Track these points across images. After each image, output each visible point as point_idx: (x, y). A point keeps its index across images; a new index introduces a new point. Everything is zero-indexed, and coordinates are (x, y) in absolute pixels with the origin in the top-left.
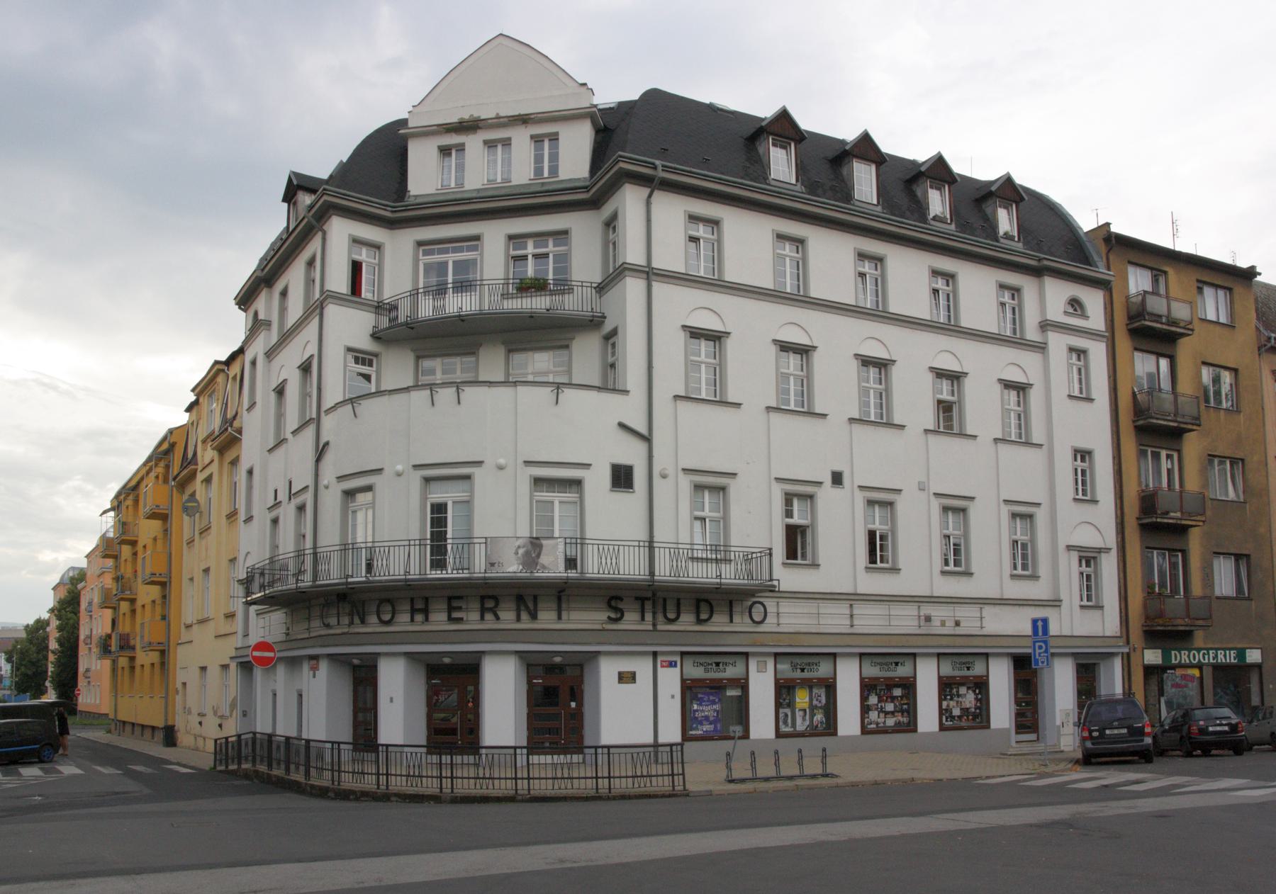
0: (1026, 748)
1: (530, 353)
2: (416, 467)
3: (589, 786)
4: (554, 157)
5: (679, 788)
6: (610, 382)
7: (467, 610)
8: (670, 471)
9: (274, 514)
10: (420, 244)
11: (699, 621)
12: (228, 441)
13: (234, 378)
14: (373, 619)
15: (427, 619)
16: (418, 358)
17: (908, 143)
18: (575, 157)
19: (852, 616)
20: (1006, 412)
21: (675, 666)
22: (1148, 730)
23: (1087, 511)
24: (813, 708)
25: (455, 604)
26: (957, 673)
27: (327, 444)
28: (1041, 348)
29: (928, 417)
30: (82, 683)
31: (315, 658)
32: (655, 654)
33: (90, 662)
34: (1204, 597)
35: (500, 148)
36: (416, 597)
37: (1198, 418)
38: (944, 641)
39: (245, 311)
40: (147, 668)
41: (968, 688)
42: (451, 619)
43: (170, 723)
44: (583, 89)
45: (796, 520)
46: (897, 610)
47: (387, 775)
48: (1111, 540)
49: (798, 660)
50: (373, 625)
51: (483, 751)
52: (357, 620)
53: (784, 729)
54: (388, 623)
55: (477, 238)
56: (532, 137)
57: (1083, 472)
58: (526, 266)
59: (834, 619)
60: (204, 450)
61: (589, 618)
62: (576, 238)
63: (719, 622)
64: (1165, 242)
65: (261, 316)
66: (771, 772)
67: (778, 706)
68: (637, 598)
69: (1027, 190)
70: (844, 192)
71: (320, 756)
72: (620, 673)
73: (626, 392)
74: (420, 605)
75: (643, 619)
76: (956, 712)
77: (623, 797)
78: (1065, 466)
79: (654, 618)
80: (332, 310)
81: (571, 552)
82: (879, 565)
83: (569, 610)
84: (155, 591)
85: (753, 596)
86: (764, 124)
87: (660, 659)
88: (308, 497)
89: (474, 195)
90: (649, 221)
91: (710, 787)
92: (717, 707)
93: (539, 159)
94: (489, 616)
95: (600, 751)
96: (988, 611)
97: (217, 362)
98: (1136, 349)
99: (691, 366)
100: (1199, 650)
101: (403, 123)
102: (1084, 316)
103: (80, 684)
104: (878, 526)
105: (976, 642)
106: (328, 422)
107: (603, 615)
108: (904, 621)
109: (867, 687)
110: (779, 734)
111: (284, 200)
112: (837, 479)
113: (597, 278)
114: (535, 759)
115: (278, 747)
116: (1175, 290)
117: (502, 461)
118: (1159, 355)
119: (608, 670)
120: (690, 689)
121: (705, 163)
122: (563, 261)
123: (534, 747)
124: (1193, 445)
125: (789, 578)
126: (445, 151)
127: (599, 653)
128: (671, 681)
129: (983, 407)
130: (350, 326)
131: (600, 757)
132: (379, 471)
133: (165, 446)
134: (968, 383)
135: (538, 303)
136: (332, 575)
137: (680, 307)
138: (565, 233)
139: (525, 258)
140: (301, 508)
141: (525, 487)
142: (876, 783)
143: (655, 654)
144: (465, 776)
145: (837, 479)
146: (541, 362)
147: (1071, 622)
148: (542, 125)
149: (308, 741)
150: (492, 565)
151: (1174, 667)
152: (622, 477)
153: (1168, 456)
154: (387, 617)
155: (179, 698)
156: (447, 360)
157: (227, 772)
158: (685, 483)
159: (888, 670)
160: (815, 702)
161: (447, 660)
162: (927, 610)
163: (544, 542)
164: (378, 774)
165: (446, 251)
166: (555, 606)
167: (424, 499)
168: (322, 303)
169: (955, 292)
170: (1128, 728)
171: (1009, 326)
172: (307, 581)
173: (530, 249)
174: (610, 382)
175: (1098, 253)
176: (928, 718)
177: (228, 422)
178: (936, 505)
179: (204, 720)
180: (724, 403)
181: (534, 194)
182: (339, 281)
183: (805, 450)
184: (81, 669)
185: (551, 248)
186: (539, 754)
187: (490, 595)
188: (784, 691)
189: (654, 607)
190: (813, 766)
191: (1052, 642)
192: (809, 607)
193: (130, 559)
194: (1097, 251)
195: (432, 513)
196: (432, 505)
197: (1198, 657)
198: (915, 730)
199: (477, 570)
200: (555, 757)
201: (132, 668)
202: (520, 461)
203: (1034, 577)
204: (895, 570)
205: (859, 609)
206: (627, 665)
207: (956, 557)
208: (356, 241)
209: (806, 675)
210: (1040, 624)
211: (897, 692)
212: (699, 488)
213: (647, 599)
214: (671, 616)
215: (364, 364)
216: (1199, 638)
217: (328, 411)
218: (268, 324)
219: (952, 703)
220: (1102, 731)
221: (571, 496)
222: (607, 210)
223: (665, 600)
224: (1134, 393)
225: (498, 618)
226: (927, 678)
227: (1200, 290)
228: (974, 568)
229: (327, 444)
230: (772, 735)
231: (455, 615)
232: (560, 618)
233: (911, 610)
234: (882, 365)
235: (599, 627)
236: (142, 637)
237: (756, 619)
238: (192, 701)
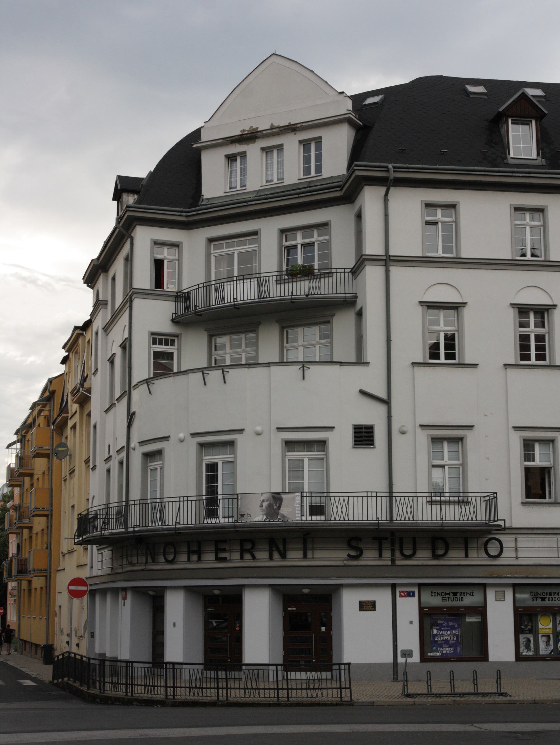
2: (194, 435)
7: (230, 551)
11: (435, 557)
15: (199, 559)
16: (210, 337)
21: (413, 596)
25: (221, 546)
31: (124, 589)
39: (92, 288)
42: (218, 559)
43: (50, 643)
49: (540, 590)
51: (244, 667)
53: (524, 652)
55: (255, 233)
61: (335, 556)
62: (335, 228)
63: (455, 557)
66: (470, 689)
67: (518, 631)
68: (374, 538)
72: (361, 602)
75: (380, 555)
79: (393, 554)
80: (137, 303)
81: (317, 501)
83: (313, 549)
90: (386, 215)
91: (375, 699)
94: (247, 556)
106: (135, 394)
107: (343, 554)
110: (519, 657)
114: (292, 675)
117: (259, 429)
119: (349, 600)
120: (427, 616)
123: (290, 664)
127: (341, 586)
128: (409, 609)
131: (343, 671)
132: (166, 438)
135: (300, 289)
138: (326, 225)
140: (121, 463)
141: (277, 448)
142: (535, 702)
143: (394, 587)
146: (306, 339)
150: (242, 516)
152: (363, 436)
154: (171, 557)
155: (57, 619)
157: (57, 685)
158: (423, 437)
163: (283, 496)
164: (126, 684)
166: (301, 546)
173: (299, 239)
185: (316, 237)
186: (295, 671)
187: (246, 539)
188: (525, 618)
201: (30, 590)
206: (367, 595)
212: (436, 440)
213: (386, 539)
214: (408, 552)
217: (137, 385)
221: (315, 454)
223: (401, 539)
225: (254, 557)
230: (511, 657)
232: (305, 556)
237: (493, 552)
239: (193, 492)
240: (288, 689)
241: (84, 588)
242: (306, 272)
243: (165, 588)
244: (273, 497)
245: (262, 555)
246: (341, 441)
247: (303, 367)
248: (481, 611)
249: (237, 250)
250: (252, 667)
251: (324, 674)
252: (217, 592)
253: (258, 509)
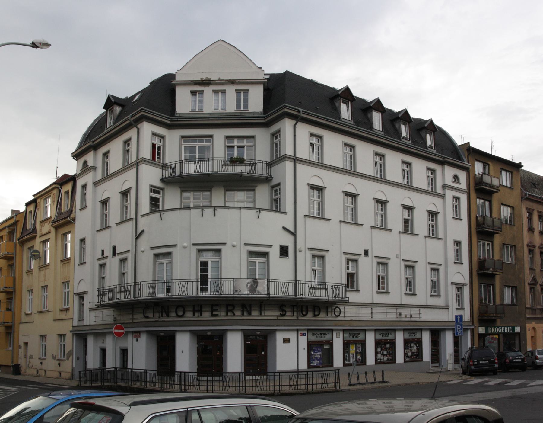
0: (436, 370)
1: (236, 192)
2: (194, 245)
3: (271, 389)
4: (246, 101)
6: (276, 206)
7: (220, 311)
8: (303, 249)
9: (102, 262)
10: (183, 137)
11: (315, 316)
12: (64, 222)
14: (173, 314)
15: (201, 315)
16: (182, 191)
18: (256, 102)
19: (372, 313)
20: (376, 214)
22: (496, 361)
23: (458, 267)
24: (356, 353)
25: (214, 308)
26: (411, 337)
28: (443, 196)
29: (400, 227)
32: (297, 330)
34: (500, 305)
35: (220, 94)
36: (196, 305)
37: (501, 228)
38: (406, 324)
41: (414, 344)
42: (213, 315)
44: (260, 70)
45: (351, 271)
47: (185, 385)
48: (467, 281)
50: (173, 317)
52: (164, 315)
54: (182, 316)
55: (211, 136)
56: (236, 90)
58: (234, 151)
59: (365, 314)
61: (271, 314)
63: (322, 316)
64: (489, 151)
65: (90, 164)
68: (291, 306)
69: (439, 128)
70: (369, 124)
72: (284, 339)
73: (286, 213)
76: (410, 354)
77: (318, 393)
78: (451, 247)
79: (297, 314)
83: (264, 310)
85: (335, 304)
86: (339, 93)
87: (299, 332)
88: (130, 257)
89: (208, 116)
90: (295, 135)
92: (320, 353)
93: (238, 101)
95: (276, 374)
96: (423, 311)
98: (478, 198)
99: (311, 202)
100: (498, 327)
102: (459, 183)
104: (381, 274)
105: (418, 324)
107: (278, 313)
108: (391, 315)
109: (378, 343)
112: (366, 253)
113: (268, 160)
114: (248, 378)
116: (492, 173)
117: (235, 243)
118: (486, 200)
119: (280, 337)
120: (311, 346)
121: (316, 110)
124: (497, 239)
125: (353, 297)
126: (193, 93)
127: (276, 330)
128: (303, 341)
129: (421, 222)
130: (151, 175)
131: (276, 377)
134: (415, 211)
136: (144, 294)
137: (308, 175)
138: (253, 137)
139: (233, 147)
141: (244, 255)
143: (297, 330)
145: (366, 253)
148: (241, 85)
150: (236, 291)
151: (489, 334)
153: (488, 244)
154: (181, 314)
156: (195, 193)
158: (309, 254)
159: (385, 336)
160: (357, 351)
161: (209, 333)
162: (400, 310)
163: (259, 281)
165: (195, 141)
167: (197, 259)
168: (138, 163)
169: (411, 171)
170: (489, 360)
171: (379, 173)
174: (276, 206)
175: (464, 155)
176: (400, 357)
178: (403, 264)
180: (323, 219)
182: (146, 153)
183: (355, 240)
185: (245, 143)
189: (297, 309)
191: (463, 324)
194: (464, 154)
195: (201, 266)
196: (201, 262)
197: (498, 330)
198: (395, 362)
199: (224, 293)
200: (257, 377)
202: (243, 243)
203: (439, 296)
204: (387, 293)
205: (375, 310)
206: (287, 335)
207: (410, 287)
208: (154, 134)
209: (355, 339)
210: (459, 317)
211: (388, 346)
214: (304, 313)
215: (157, 193)
216: (498, 322)
217: (143, 216)
219: (408, 351)
220: (478, 362)
222: (274, 128)
224: (477, 217)
225: (234, 314)
226: (400, 339)
227: (501, 172)
228: (417, 292)
231: (215, 313)
232: (261, 314)
233: (393, 311)
234: (354, 196)
235: (276, 318)
239: (193, 276)
240: (279, 386)
241: (122, 331)
242: (240, 161)
243: (176, 331)
244: (254, 281)
246: (274, 253)
247: (259, 211)
248: (331, 343)
250: (233, 374)
253: (245, 288)
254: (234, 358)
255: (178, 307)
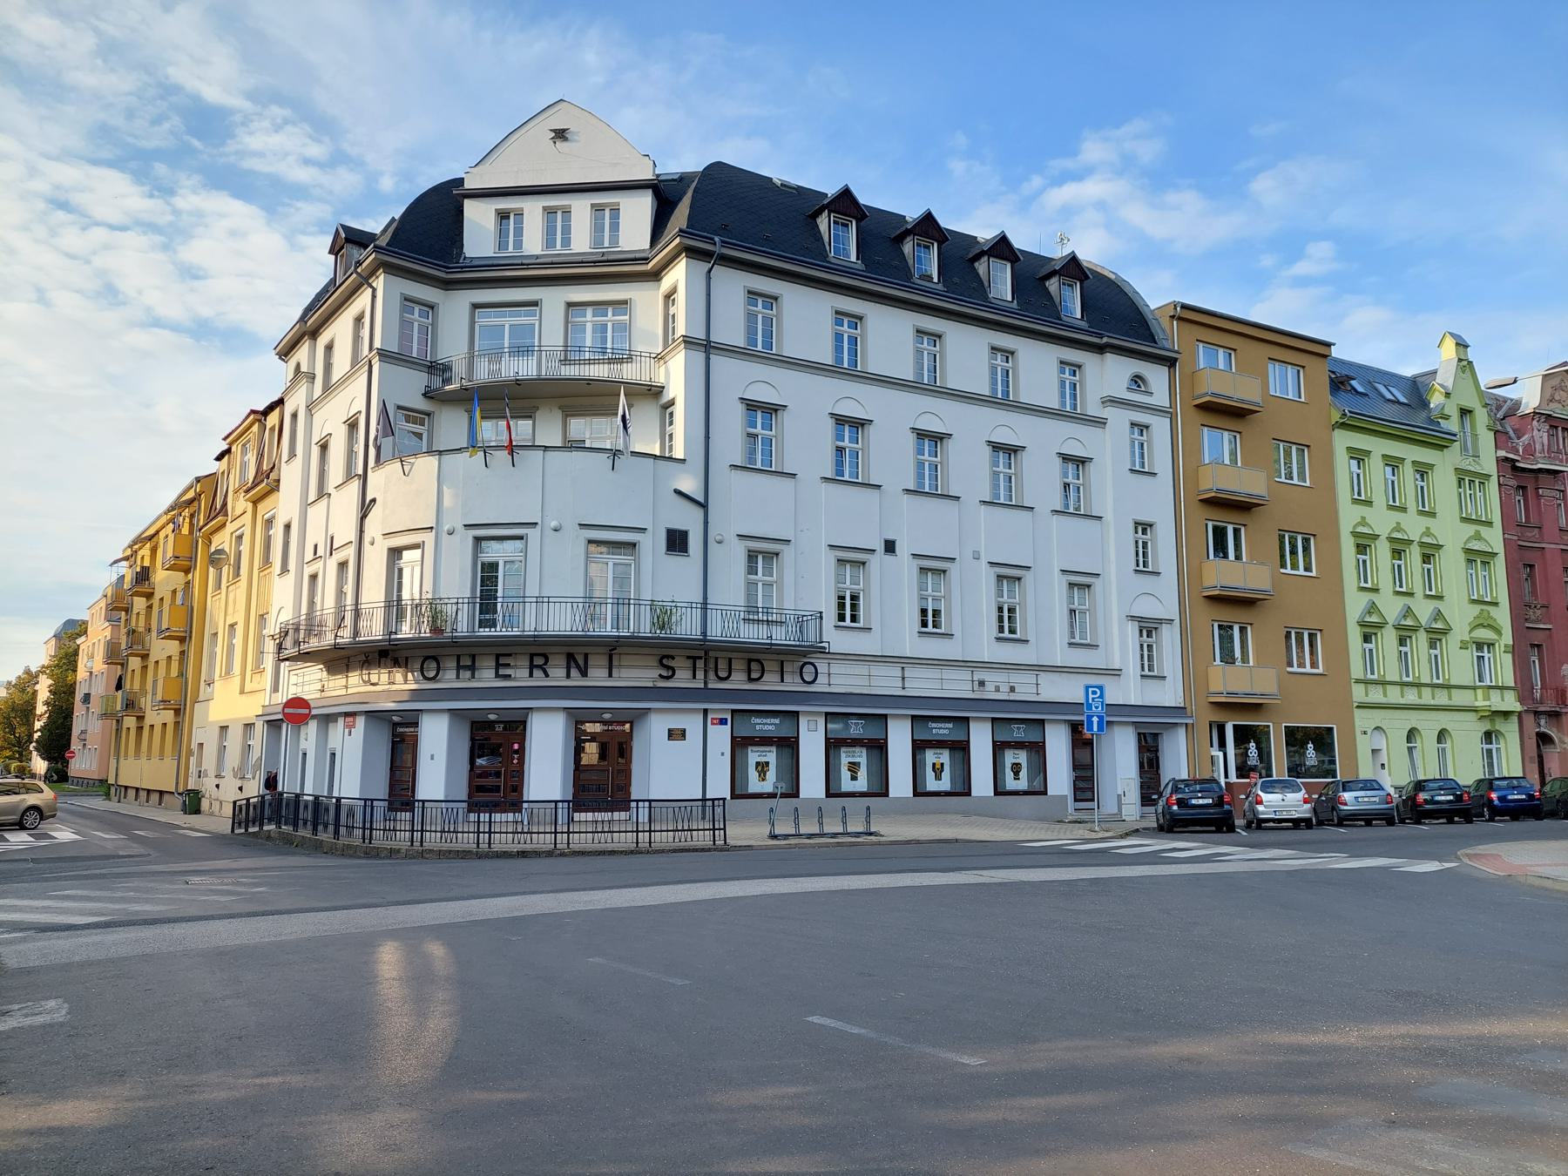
5: (720, 842)
7: (515, 667)
11: (750, 680)
13: (272, 429)
17: (977, 223)
23: (1146, 582)
27: (374, 500)
30: (75, 745)
32: (706, 711)
33: (86, 723)
40: (158, 730)
46: (950, 674)
55: (535, 304)
57: (1145, 545)
59: (885, 682)
60: (235, 500)
71: (351, 813)
74: (467, 662)
82: (930, 628)
84: (173, 647)
94: (538, 673)
96: (1044, 678)
97: (253, 412)
101: (460, 181)
103: (73, 747)
107: (655, 673)
108: (958, 685)
111: (330, 252)
112: (890, 547)
115: (306, 807)
122: (624, 329)
125: (838, 640)
128: (721, 737)
133: (191, 494)
144: (503, 829)
147: (1129, 691)
149: (339, 800)
154: (432, 674)
166: (605, 662)
172: (346, 636)
177: (261, 475)
179: (221, 782)
181: (595, 263)
184: (75, 732)
187: (538, 651)
190: (856, 826)
192: (862, 669)
193: (143, 612)
196: (483, 564)
206: (677, 722)
214: (723, 674)
218: (312, 377)
229: (374, 500)
230: (823, 795)
231: (501, 672)
232: (610, 675)
233: (965, 675)
235: (650, 684)
236: (154, 694)
238: (209, 763)
245: (557, 676)
249: (507, 320)
251: (616, 814)
252: (492, 717)
254: (546, 769)
255: (426, 658)
